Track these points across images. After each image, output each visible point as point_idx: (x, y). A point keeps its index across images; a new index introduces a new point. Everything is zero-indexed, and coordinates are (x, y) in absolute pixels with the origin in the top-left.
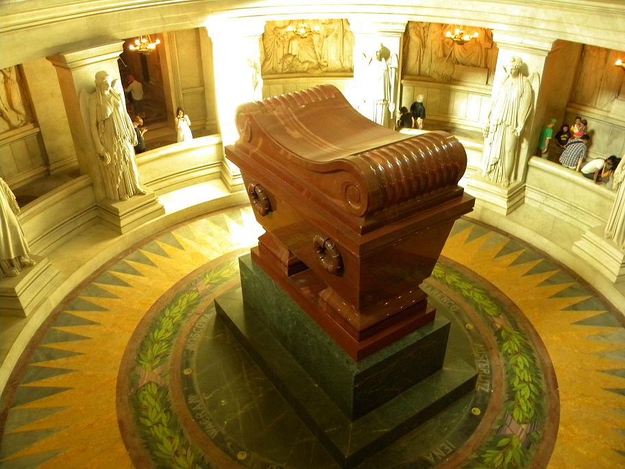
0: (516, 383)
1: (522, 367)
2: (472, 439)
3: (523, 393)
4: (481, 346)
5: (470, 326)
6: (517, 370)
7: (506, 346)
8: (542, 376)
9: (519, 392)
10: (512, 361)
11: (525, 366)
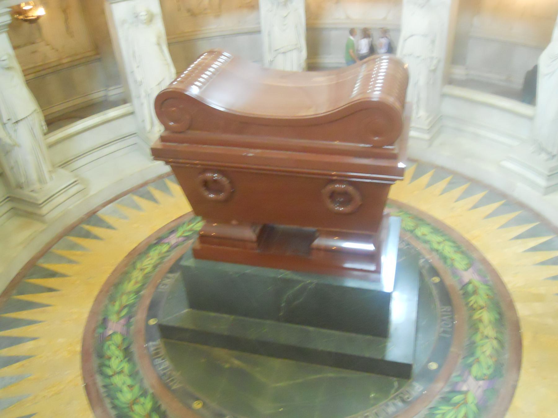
0: (126, 367)
1: (125, 389)
2: (147, 302)
3: (117, 361)
4: (174, 387)
5: (197, 405)
6: (129, 381)
7: (149, 405)
8: (102, 390)
9: (122, 358)
10: (136, 389)
11: (121, 391)
